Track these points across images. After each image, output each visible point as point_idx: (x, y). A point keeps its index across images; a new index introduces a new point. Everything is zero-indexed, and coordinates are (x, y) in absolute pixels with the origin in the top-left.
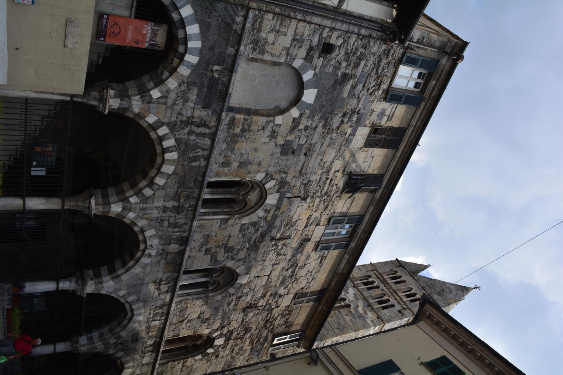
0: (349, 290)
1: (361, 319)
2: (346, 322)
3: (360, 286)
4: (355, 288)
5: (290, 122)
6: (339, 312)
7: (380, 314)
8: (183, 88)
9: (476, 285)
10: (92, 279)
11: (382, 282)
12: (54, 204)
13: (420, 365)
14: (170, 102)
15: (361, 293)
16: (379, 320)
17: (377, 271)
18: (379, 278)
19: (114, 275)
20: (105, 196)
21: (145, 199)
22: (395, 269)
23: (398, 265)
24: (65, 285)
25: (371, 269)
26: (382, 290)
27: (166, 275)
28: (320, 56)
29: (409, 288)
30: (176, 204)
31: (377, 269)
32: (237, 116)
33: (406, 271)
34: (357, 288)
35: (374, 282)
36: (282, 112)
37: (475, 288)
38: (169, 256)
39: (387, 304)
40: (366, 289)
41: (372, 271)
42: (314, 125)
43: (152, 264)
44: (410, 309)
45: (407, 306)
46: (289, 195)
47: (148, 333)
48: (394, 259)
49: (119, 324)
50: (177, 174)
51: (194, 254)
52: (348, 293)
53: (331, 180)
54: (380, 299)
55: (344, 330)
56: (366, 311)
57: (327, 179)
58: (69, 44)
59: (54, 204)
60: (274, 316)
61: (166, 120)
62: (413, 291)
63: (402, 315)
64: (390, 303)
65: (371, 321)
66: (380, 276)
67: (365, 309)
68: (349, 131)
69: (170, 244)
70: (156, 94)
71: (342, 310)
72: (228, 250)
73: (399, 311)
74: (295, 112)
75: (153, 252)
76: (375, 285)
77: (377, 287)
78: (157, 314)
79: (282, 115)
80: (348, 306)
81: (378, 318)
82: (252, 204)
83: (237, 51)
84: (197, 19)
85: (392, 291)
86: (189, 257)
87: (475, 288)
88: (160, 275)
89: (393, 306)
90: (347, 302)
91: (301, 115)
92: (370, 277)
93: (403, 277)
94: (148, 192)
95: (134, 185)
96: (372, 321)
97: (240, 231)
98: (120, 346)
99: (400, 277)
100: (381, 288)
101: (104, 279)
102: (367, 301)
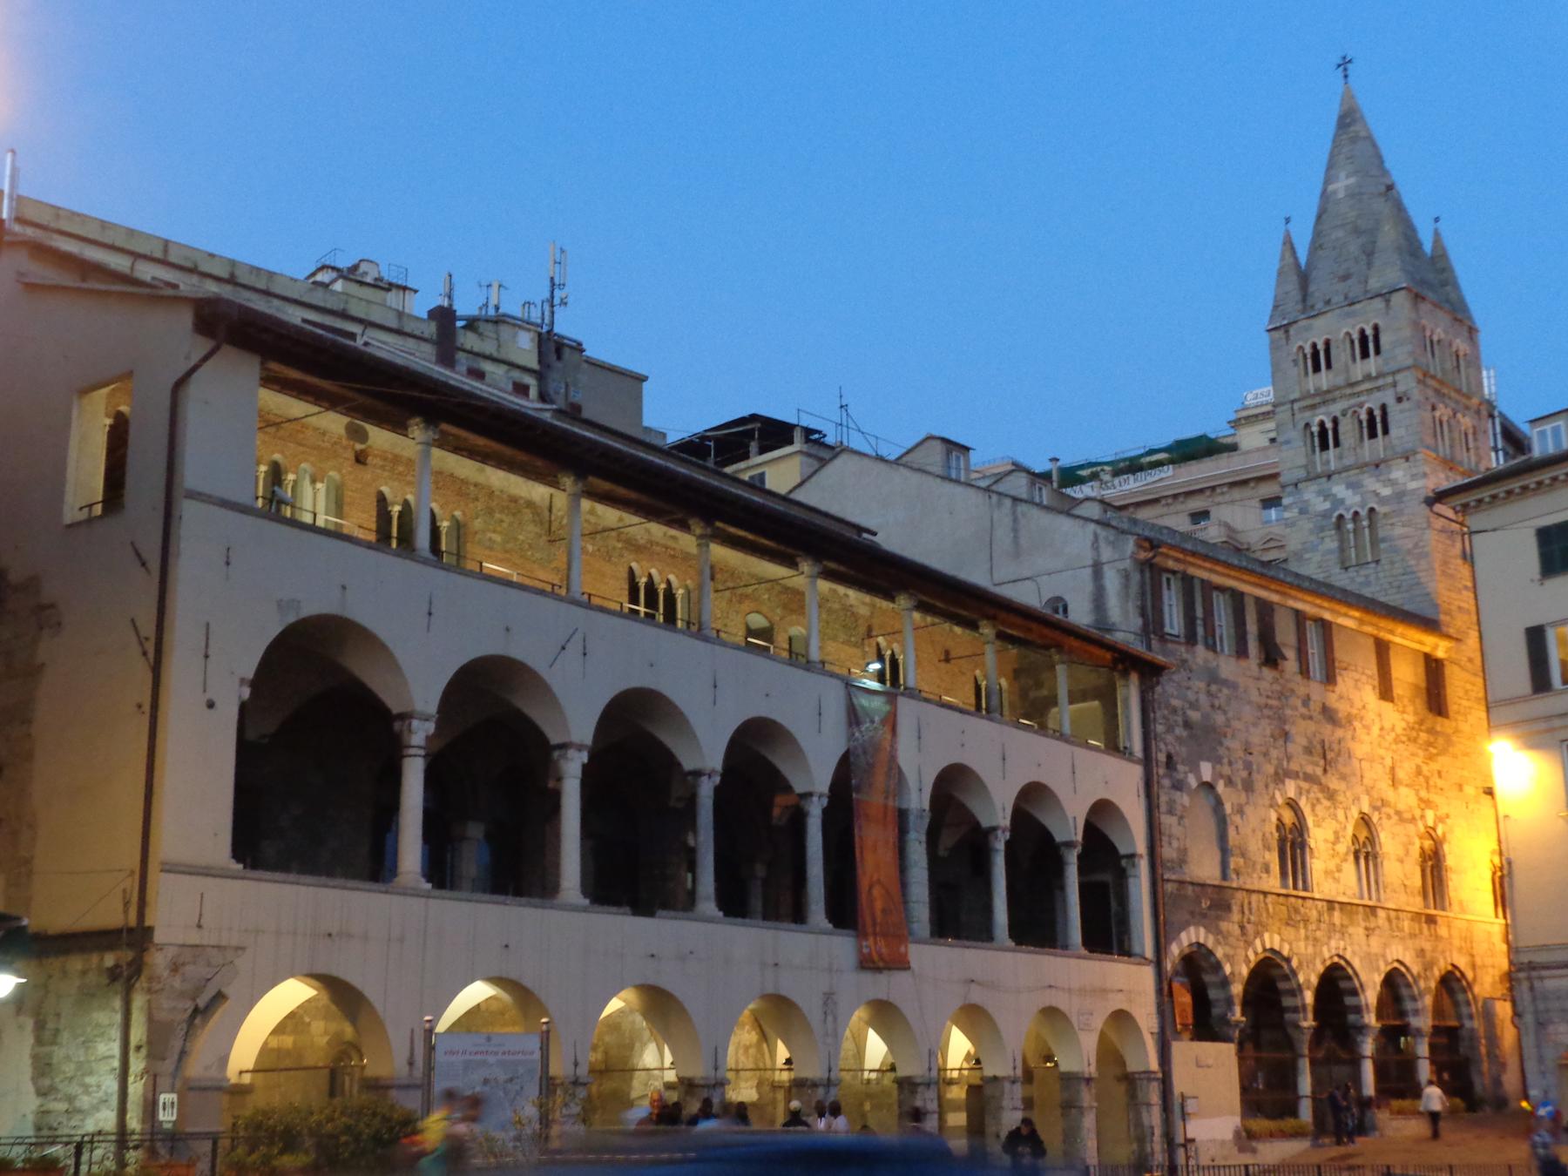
0: (1335, 495)
1: (1405, 499)
2: (1407, 537)
3: (1328, 462)
4: (1335, 477)
5: (1229, 790)
6: (1384, 540)
7: (1399, 449)
8: (1221, 940)
9: (1339, 66)
10: (1362, 1017)
11: (1324, 403)
12: (1305, 1065)
13: (1542, 584)
14: (1231, 952)
15: (1347, 469)
16: (1411, 459)
17: (1293, 402)
18: (1313, 407)
19: (1360, 990)
20: (1295, 1010)
21: (1300, 963)
22: (1295, 350)
23: (1279, 334)
24: (1368, 1047)
25: (1289, 413)
26: (1344, 414)
27: (1363, 924)
28: (1175, 769)
29: (1345, 338)
30: (1302, 925)
31: (1292, 397)
32: (1232, 866)
33: (1301, 324)
34: (1334, 473)
35: (1322, 424)
36: (1218, 804)
37: (1346, 76)
38: (1346, 922)
39: (1378, 419)
40: (1338, 450)
41: (1293, 415)
42: (1227, 752)
43: (1352, 944)
44: (1399, 371)
45: (1388, 374)
46: (1285, 763)
47: (1415, 935)
48: (1265, 339)
49: (1403, 975)
50: (1279, 929)
51: (1341, 890)
52: (1342, 501)
53: (1268, 697)
54: (1365, 431)
55: (1424, 546)
56: (1389, 480)
57: (1266, 706)
58: (1210, 1062)
59: (1305, 1065)
60: (1405, 729)
61: (1244, 953)
62: (1356, 336)
63: (1408, 399)
64: (1377, 413)
65: (1413, 480)
66: (1309, 402)
67: (1382, 478)
68: (1225, 691)
69: (1334, 925)
70: (1228, 969)
71: (1381, 533)
72: (1337, 840)
73: (1399, 400)
74: (1221, 787)
75: (1342, 944)
76: (1329, 425)
77: (1335, 421)
78: (1398, 927)
79: (1223, 804)
80: (1372, 510)
81: (1407, 459)
82: (1293, 814)
83: (1192, 884)
84: (1176, 937)
85: (1348, 391)
86: (1344, 894)
87: (1346, 76)
88: (1361, 931)
89: (1384, 408)
90: (1363, 513)
91: (1221, 776)
92: (1307, 425)
93: (1316, 340)
94: (1294, 963)
95: (1286, 978)
96: (1414, 477)
97: (1319, 826)
98: (1428, 973)
99: (1314, 346)
100: (1338, 414)
101: (1363, 1002)
102: (1366, 465)
